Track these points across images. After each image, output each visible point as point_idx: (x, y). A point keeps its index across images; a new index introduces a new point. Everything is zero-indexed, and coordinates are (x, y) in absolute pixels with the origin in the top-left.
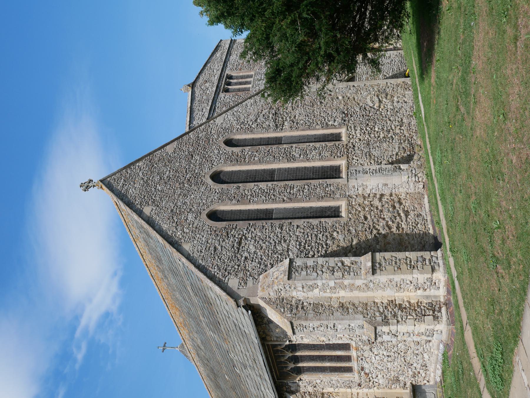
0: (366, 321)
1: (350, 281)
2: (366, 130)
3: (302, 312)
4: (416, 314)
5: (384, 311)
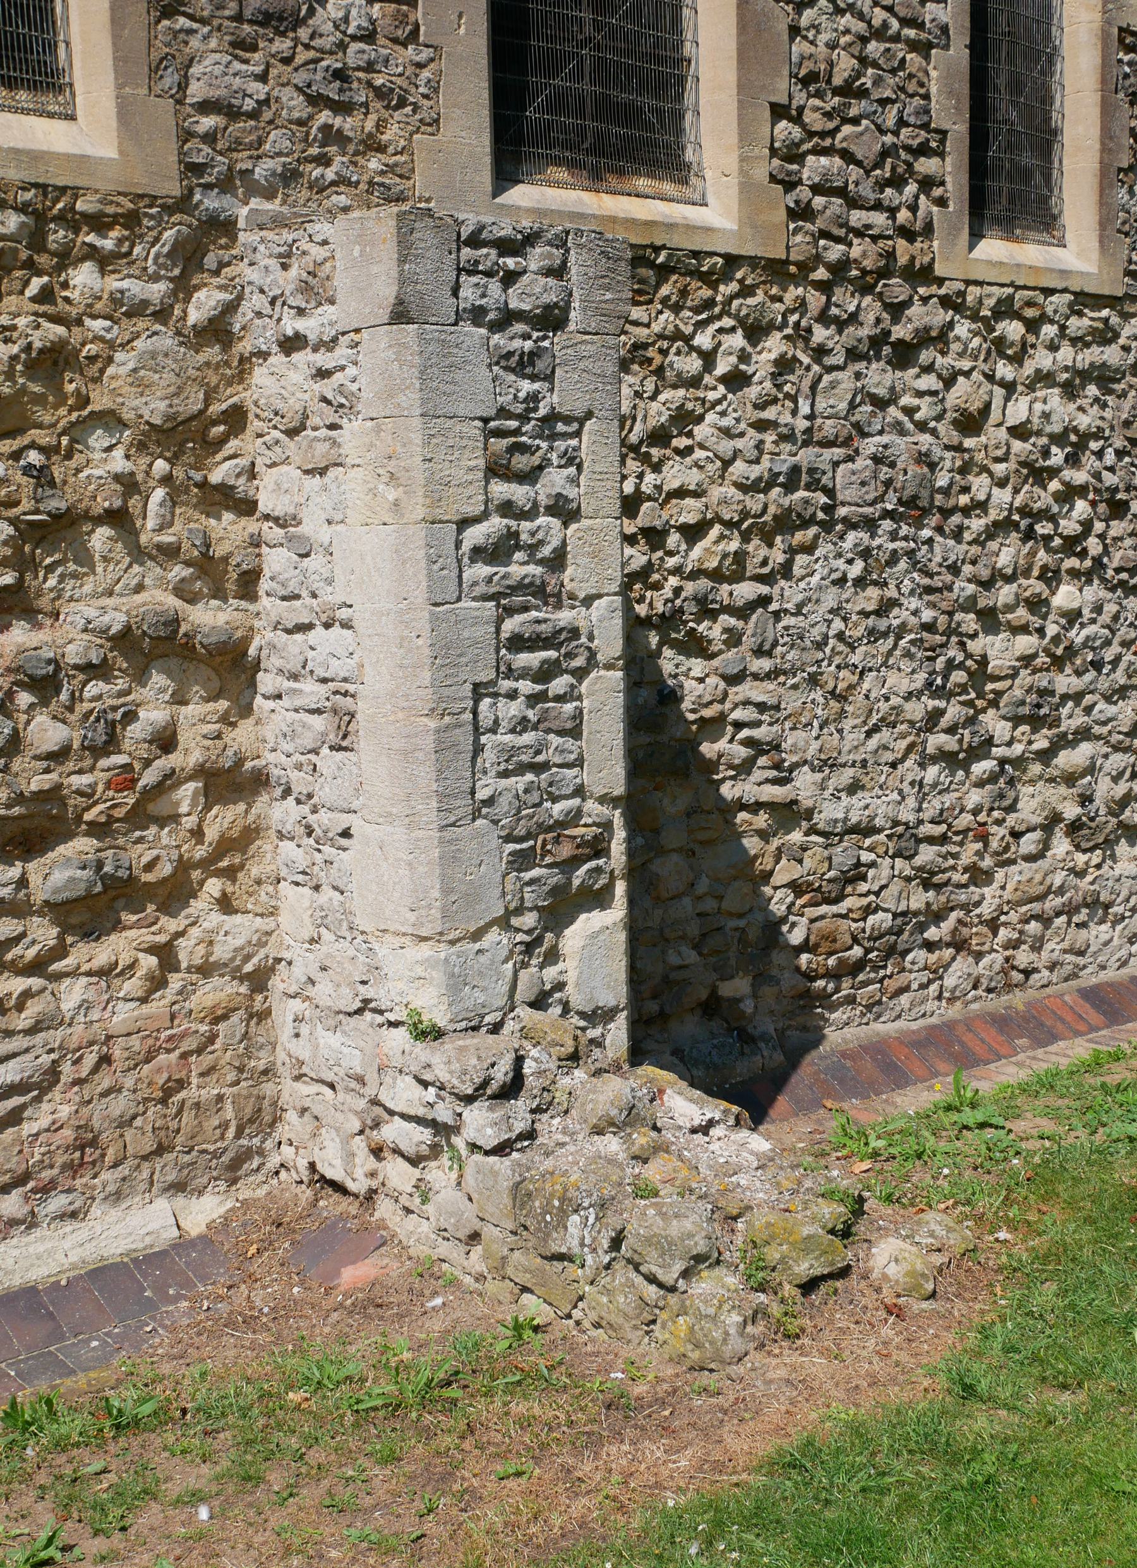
2: (1069, 494)
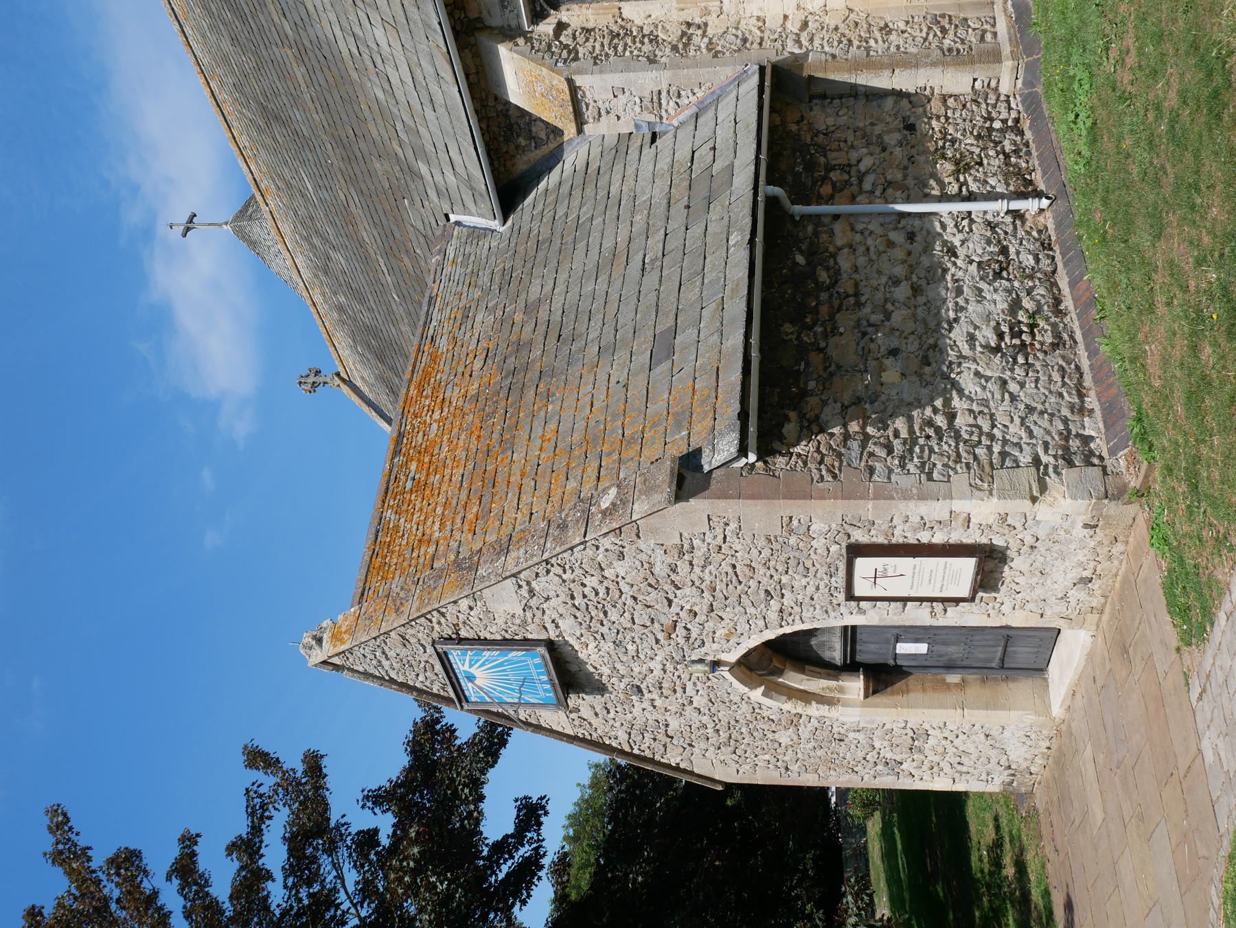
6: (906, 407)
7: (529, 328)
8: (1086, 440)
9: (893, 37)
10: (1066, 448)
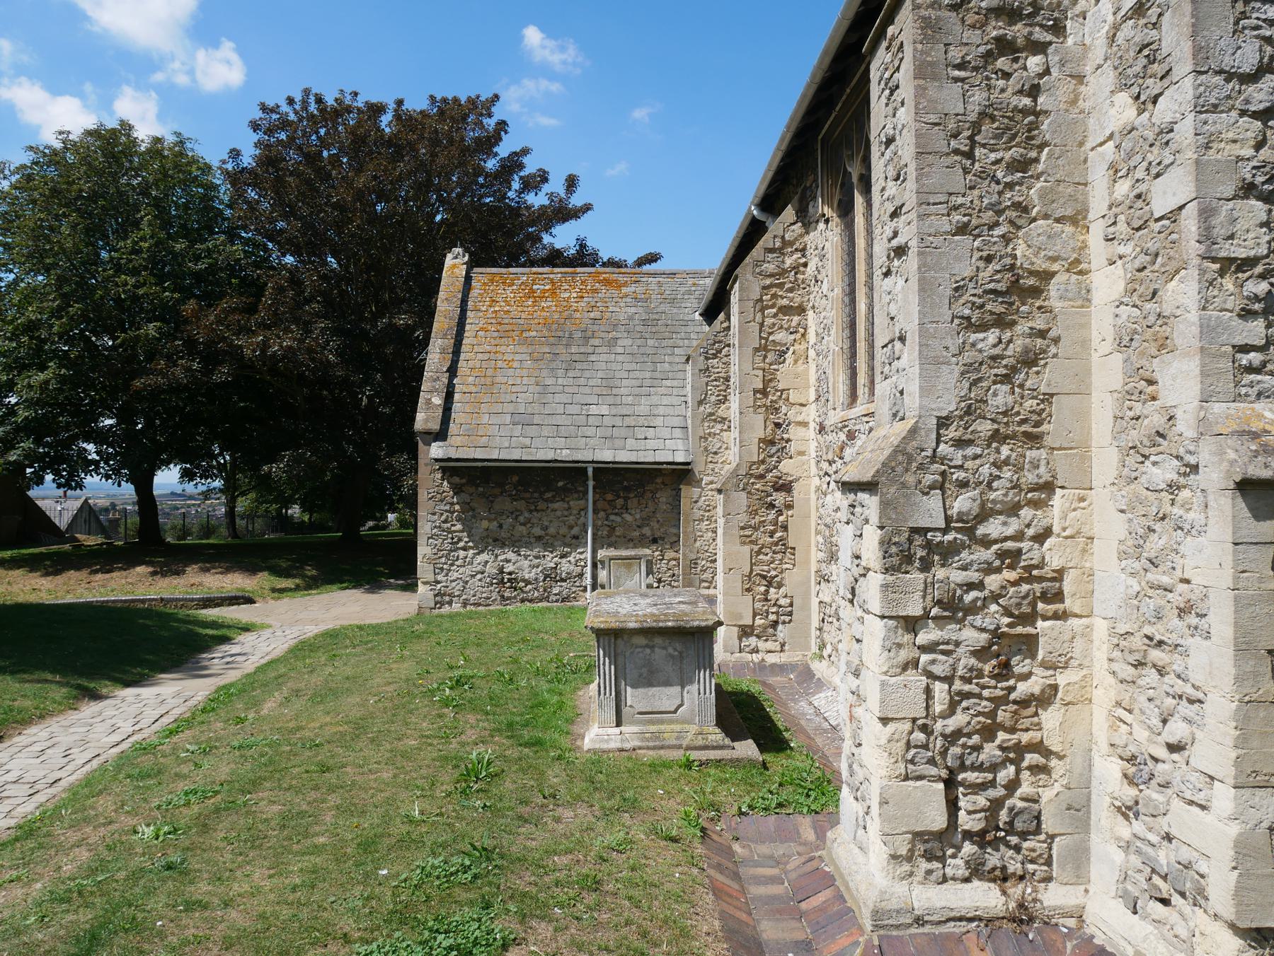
0: (913, 431)
1: (1194, 316)
3: (976, 41)
4: (958, 733)
5: (986, 542)
6: (468, 529)
7: (596, 342)
8: (450, 603)
9: (710, 534)
10: (444, 594)
